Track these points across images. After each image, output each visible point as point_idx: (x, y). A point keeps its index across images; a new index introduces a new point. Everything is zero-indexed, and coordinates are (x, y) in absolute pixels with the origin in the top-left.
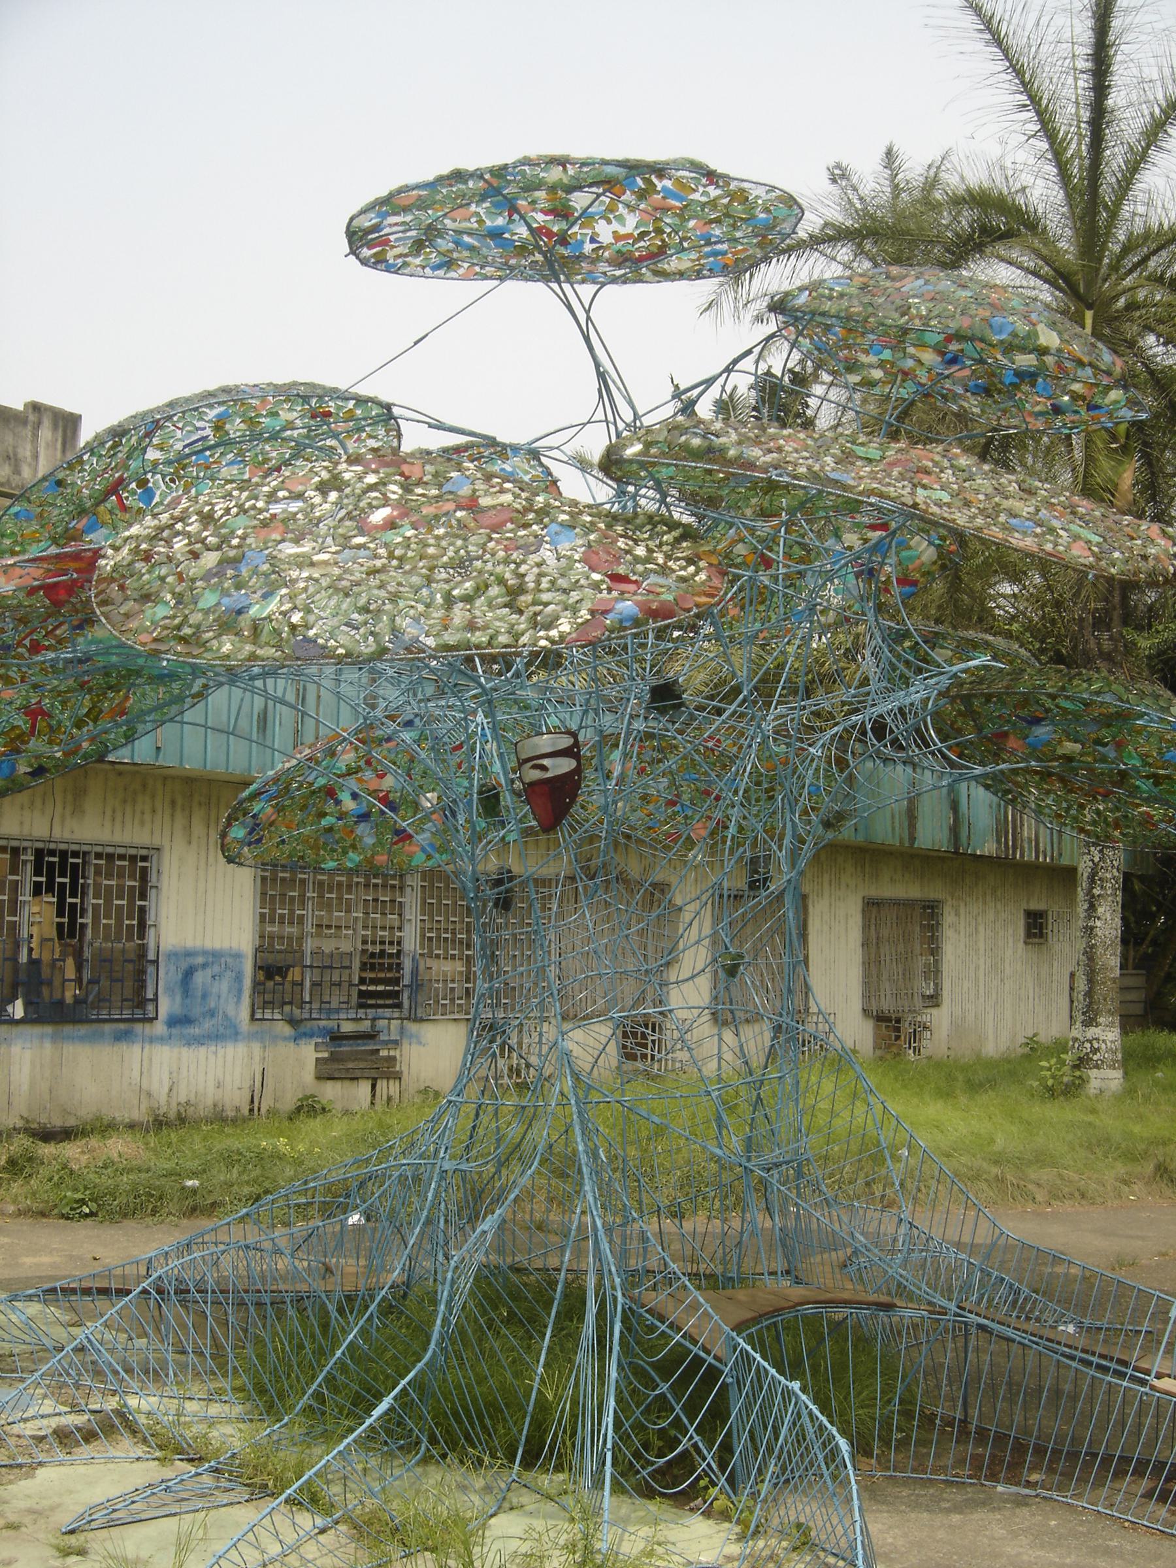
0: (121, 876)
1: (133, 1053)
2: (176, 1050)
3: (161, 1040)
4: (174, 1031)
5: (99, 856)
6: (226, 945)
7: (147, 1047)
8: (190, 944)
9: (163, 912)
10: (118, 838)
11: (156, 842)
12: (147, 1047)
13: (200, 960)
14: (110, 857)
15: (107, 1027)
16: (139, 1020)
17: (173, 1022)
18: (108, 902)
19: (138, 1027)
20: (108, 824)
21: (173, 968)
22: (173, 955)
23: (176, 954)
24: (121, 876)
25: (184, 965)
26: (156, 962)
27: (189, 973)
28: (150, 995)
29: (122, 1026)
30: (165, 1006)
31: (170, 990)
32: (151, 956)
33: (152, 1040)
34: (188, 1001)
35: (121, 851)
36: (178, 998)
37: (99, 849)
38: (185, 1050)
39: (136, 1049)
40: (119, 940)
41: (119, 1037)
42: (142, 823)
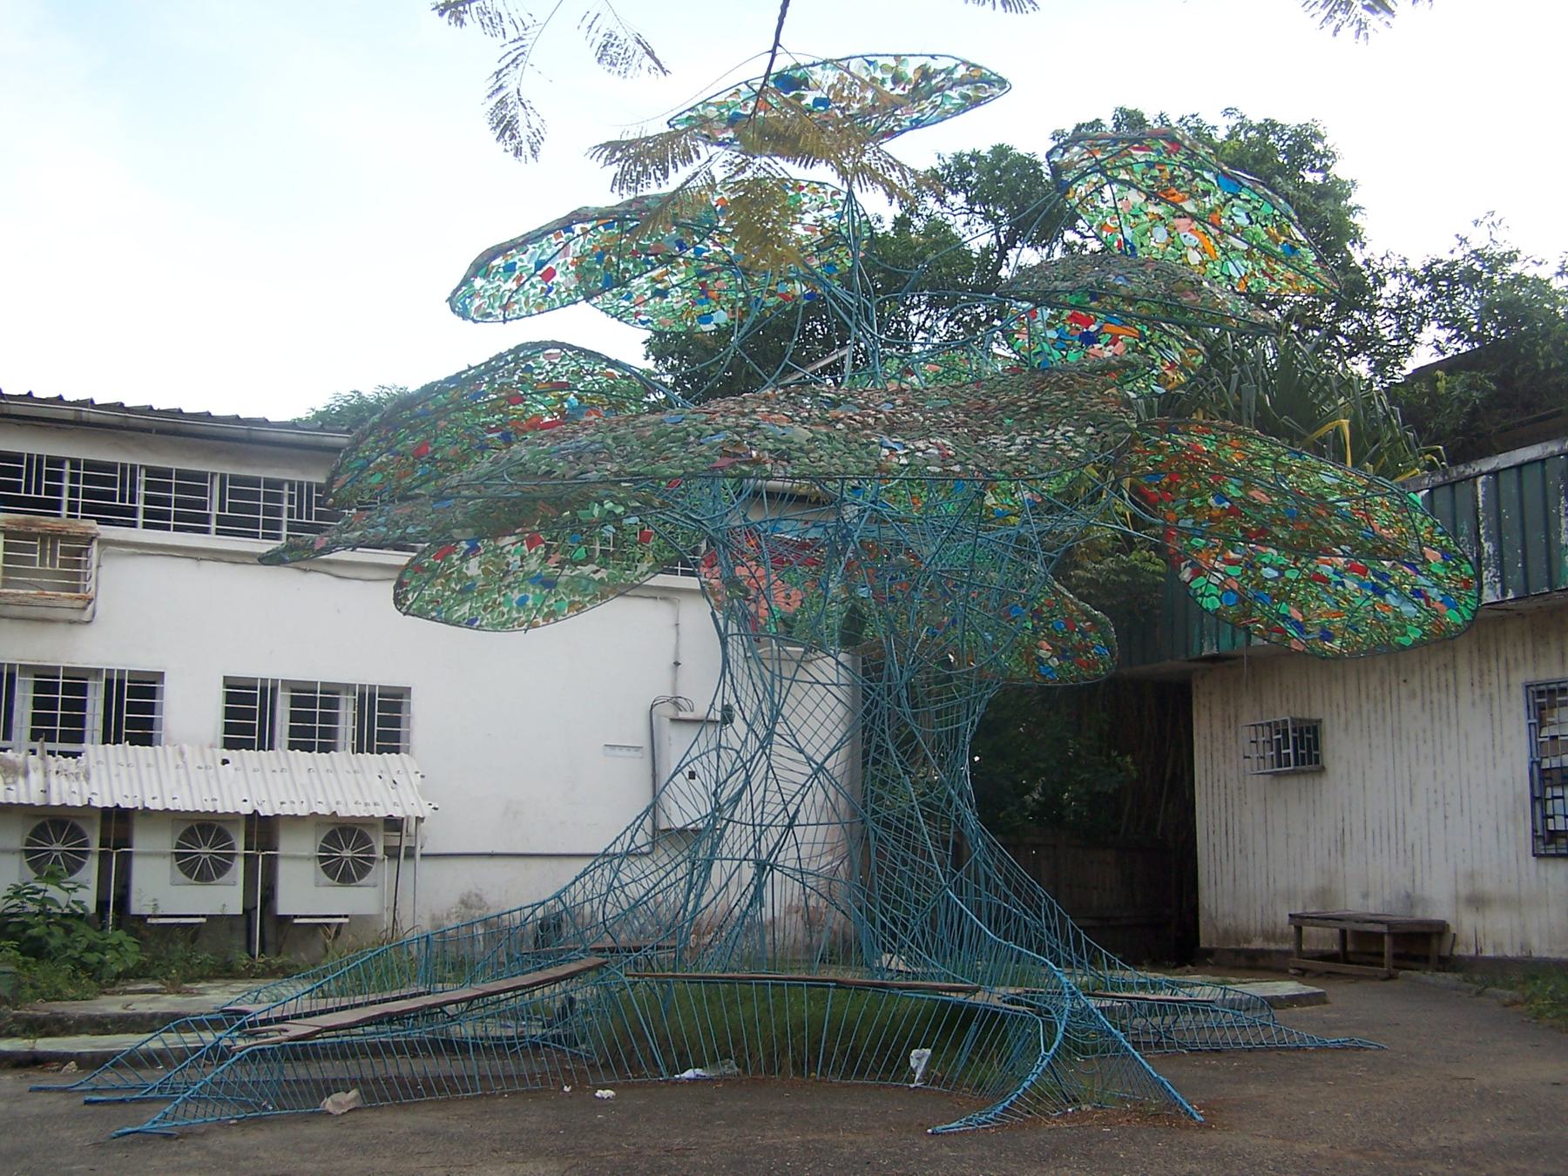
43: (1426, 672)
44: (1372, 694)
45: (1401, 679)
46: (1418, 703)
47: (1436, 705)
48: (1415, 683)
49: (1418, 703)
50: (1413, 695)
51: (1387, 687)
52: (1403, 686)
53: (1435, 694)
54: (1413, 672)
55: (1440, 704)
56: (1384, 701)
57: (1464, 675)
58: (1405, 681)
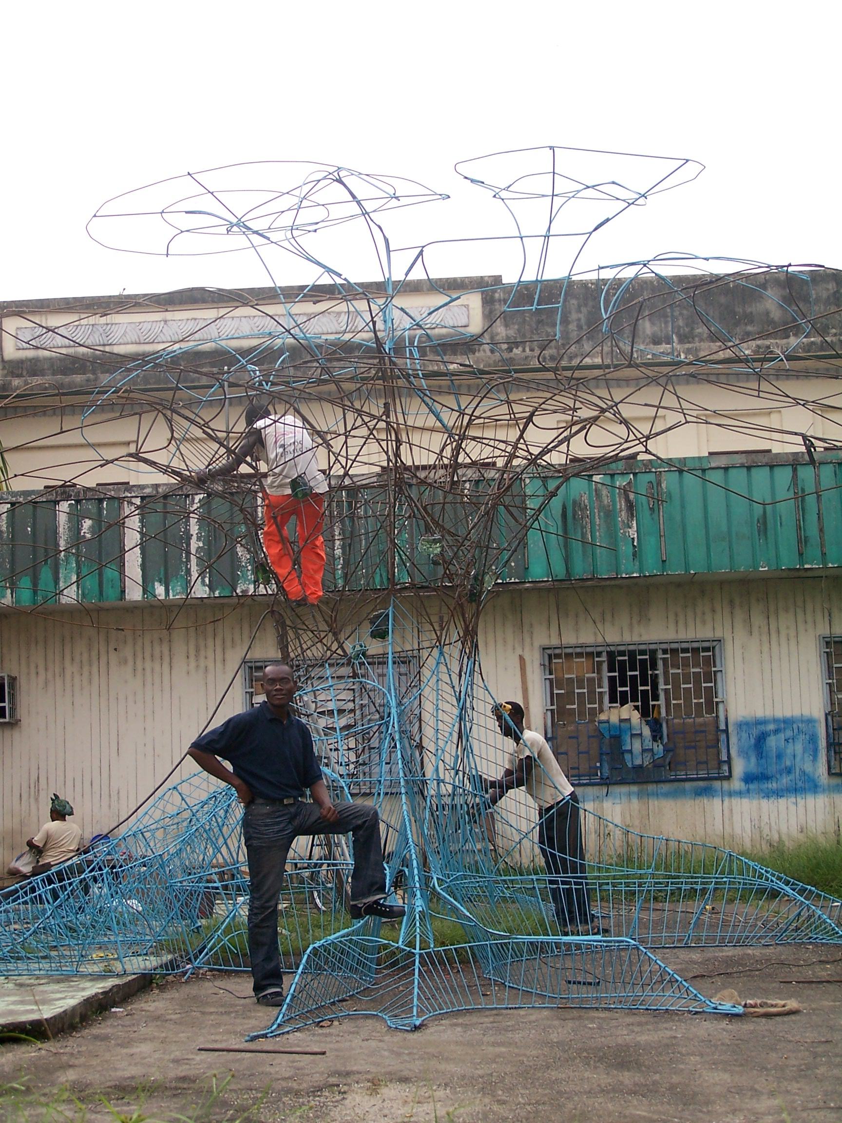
0: (686, 665)
1: (715, 806)
2: (755, 802)
3: (740, 794)
4: (752, 786)
5: (665, 651)
6: (768, 713)
7: (726, 800)
8: (760, 714)
9: (731, 689)
10: (682, 636)
11: (718, 634)
12: (726, 800)
13: (771, 727)
14: (674, 651)
15: (688, 785)
16: (716, 779)
17: (749, 778)
18: (676, 687)
19: (717, 784)
20: (672, 626)
21: (745, 735)
22: (743, 725)
23: (747, 724)
24: (686, 665)
25: (755, 732)
26: (726, 731)
27: (761, 739)
28: (724, 758)
29: (701, 784)
30: (739, 767)
31: (742, 752)
32: (722, 726)
33: (730, 794)
34: (763, 761)
35: (684, 645)
36: (753, 760)
37: (664, 646)
38: (764, 803)
39: (717, 802)
40: (689, 715)
41: (699, 793)
42: (704, 622)
43: (139, 643)
44: (77, 658)
45: (111, 649)
46: (129, 668)
47: (148, 670)
48: (128, 651)
49: (129, 668)
50: (124, 662)
51: (94, 653)
52: (113, 656)
53: (148, 665)
54: (125, 642)
55: (153, 671)
56: (90, 665)
57: (180, 648)
58: (116, 649)
